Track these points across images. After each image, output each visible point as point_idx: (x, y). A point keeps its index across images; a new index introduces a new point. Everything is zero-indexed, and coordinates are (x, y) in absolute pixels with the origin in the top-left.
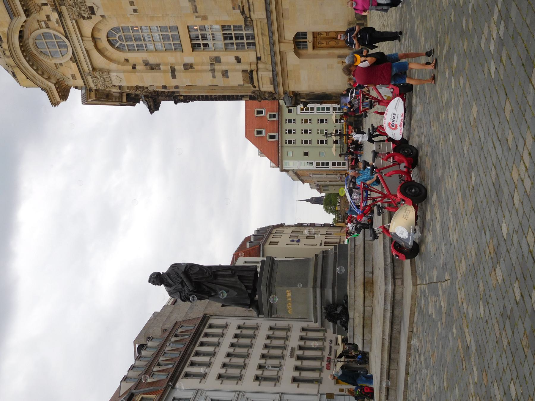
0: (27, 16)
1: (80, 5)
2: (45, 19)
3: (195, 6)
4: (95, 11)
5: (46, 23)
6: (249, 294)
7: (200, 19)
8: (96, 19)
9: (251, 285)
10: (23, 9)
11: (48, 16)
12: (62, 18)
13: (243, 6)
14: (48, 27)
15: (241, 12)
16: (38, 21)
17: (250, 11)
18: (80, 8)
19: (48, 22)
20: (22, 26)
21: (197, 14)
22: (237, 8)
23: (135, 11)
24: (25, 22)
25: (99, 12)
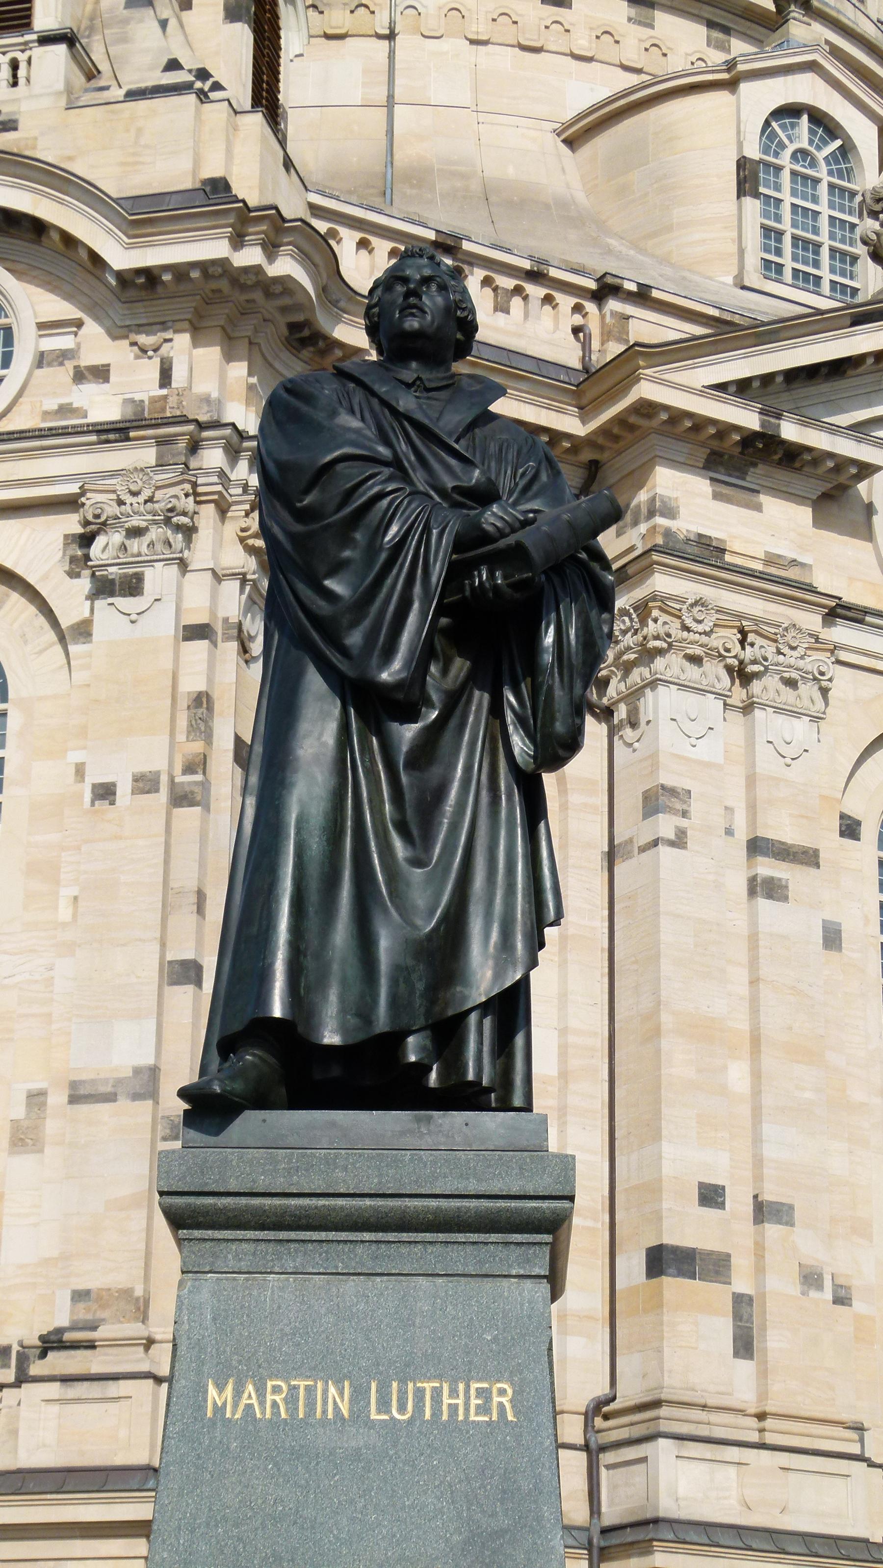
0: (125, 279)
1: (155, 533)
2: (88, 359)
3: (110, 1098)
4: (122, 602)
5: (63, 356)
6: (394, 1040)
7: (19, 1111)
8: (70, 598)
9: (471, 1076)
10: (166, 268)
11: (101, 373)
12: (93, 438)
13: (91, 1346)
14: (41, 360)
15: (60, 1331)
16: (79, 324)
17: (66, 1379)
18: (136, 532)
19: (70, 365)
20: (69, 240)
21: (57, 1099)
22: (83, 1313)
23: (105, 792)
24: (96, 259)
25: (108, 616)
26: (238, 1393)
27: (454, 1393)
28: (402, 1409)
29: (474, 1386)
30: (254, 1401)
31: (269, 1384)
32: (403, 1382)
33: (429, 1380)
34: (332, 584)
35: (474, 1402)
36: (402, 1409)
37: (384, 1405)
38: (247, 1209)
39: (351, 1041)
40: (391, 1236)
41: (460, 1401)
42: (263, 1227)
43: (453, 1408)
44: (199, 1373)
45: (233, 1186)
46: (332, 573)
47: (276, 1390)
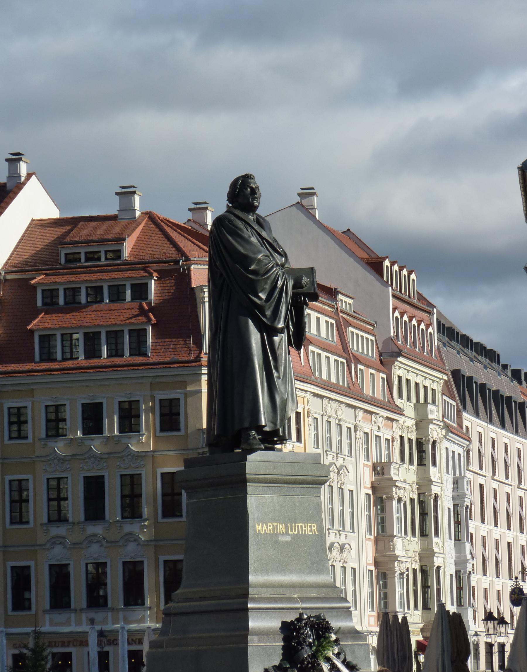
26: (262, 527)
27: (305, 527)
28: (295, 531)
29: (309, 525)
30: (266, 529)
31: (269, 524)
32: (295, 524)
33: (300, 523)
34: (260, 294)
35: (309, 529)
36: (295, 531)
37: (291, 531)
38: (265, 479)
39: (271, 430)
40: (290, 485)
41: (306, 529)
42: (266, 483)
43: (305, 530)
44: (254, 521)
45: (262, 472)
46: (261, 291)
47: (270, 526)
